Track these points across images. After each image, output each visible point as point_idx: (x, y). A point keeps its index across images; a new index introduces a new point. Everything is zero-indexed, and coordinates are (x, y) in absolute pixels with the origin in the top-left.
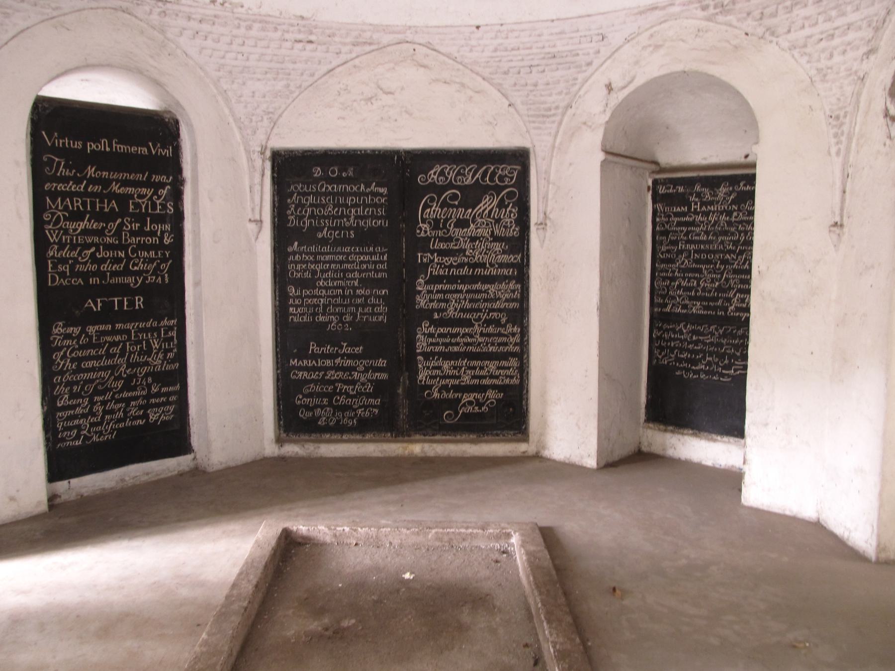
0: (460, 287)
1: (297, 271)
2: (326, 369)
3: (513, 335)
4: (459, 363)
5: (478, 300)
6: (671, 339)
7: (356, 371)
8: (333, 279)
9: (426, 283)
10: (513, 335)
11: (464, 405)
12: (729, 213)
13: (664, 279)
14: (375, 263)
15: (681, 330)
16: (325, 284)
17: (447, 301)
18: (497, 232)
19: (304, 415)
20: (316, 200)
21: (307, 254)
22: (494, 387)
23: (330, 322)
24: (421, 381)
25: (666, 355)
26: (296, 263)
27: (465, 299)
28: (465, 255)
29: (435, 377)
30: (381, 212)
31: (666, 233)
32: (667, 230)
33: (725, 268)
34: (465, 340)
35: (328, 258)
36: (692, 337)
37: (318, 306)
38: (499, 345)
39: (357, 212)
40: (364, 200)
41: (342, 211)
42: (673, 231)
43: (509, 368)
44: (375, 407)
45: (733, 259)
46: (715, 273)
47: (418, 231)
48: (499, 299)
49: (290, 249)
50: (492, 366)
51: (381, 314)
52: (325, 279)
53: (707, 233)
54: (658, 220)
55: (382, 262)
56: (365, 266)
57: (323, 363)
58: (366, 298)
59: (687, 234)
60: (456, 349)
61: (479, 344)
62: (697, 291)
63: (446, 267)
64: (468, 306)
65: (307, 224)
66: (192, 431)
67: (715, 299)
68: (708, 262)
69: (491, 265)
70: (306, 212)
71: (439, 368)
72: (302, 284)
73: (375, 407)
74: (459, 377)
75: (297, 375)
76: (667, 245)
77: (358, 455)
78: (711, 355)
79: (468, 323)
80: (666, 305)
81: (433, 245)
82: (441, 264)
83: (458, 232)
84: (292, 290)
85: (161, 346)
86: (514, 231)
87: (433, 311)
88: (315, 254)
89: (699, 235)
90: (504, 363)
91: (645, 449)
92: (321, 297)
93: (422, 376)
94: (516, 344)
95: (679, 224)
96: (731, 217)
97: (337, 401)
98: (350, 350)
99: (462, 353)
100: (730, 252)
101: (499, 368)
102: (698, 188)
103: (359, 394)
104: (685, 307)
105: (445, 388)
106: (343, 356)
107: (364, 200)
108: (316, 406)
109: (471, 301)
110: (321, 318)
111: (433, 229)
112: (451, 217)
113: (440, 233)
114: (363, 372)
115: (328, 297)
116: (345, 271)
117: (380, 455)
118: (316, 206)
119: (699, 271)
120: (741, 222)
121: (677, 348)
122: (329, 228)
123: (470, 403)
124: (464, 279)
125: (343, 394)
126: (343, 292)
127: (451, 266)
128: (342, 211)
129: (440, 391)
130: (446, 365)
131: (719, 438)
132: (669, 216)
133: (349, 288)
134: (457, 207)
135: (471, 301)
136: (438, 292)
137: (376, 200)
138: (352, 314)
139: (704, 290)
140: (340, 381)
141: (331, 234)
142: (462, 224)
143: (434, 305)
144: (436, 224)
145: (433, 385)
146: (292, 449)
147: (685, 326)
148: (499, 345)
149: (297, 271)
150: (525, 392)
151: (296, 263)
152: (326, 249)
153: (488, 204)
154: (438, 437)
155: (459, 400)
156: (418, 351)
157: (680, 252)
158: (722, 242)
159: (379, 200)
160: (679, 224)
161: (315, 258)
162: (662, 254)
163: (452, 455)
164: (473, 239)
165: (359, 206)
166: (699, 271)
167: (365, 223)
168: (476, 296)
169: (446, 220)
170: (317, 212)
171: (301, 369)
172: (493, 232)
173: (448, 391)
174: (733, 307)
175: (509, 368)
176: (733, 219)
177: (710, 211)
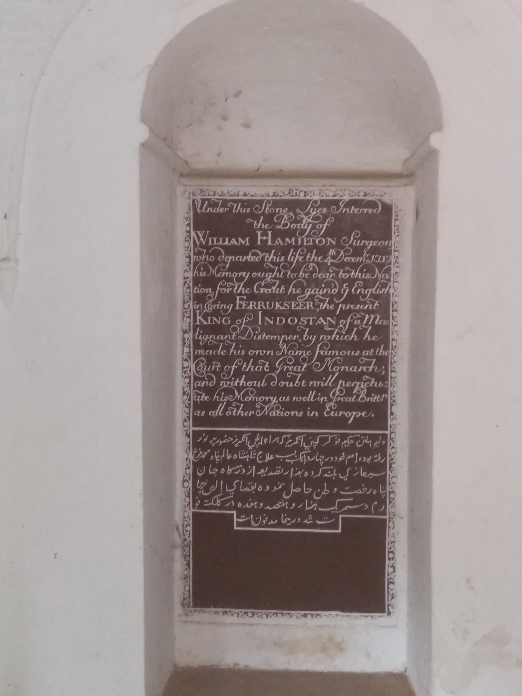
6: (225, 463)
12: (322, 251)
15: (243, 446)
25: (217, 492)
31: (210, 282)
32: (213, 276)
33: (317, 341)
36: (263, 457)
42: (225, 278)
45: (331, 325)
46: (302, 349)
53: (285, 282)
59: (250, 283)
62: (268, 381)
67: (305, 392)
68: (288, 330)
78: (298, 482)
80: (214, 405)
95: (235, 267)
96: (325, 257)
100: (325, 313)
120: (342, 265)
121: (239, 477)
132: (217, 253)
139: (282, 376)
157: (241, 313)
160: (235, 267)
166: (273, 345)
177: (290, 246)
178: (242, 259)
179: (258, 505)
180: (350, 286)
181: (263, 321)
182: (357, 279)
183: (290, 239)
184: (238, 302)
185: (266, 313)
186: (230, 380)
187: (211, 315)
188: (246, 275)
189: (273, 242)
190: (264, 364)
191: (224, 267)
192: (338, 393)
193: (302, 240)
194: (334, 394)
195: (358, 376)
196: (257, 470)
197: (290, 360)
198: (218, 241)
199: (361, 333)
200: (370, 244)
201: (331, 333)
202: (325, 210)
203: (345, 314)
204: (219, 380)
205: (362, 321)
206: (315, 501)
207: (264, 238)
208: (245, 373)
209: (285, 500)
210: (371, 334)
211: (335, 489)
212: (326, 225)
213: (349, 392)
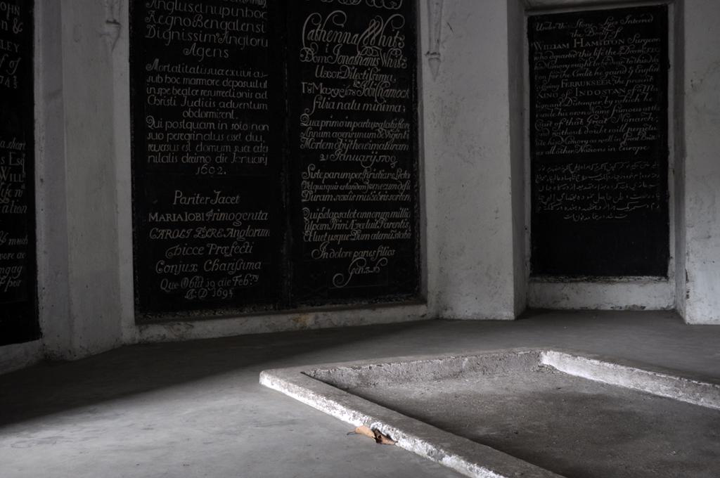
0: (348, 124)
1: (158, 97)
2: (195, 225)
3: (404, 181)
4: (348, 214)
5: (366, 141)
7: (233, 227)
8: (204, 109)
9: (312, 118)
10: (404, 181)
11: (354, 266)
12: (616, 48)
13: (546, 120)
14: (254, 90)
15: (567, 172)
16: (194, 114)
17: (334, 140)
18: (384, 62)
19: (168, 287)
20: (182, 7)
21: (170, 75)
22: (385, 242)
23: (200, 164)
24: (307, 238)
25: (552, 201)
26: (157, 86)
27: (353, 139)
28: (352, 87)
29: (320, 233)
30: (261, 29)
34: (353, 187)
35: (197, 81)
36: (580, 178)
37: (185, 142)
38: (390, 192)
39: (231, 26)
40: (240, 12)
41: (214, 23)
43: (399, 220)
44: (255, 272)
46: (603, 109)
47: (302, 55)
48: (388, 139)
49: (149, 68)
50: (382, 217)
51: (260, 155)
52: (194, 109)
53: (592, 69)
54: (535, 58)
55: (262, 91)
56: (241, 95)
57: (192, 217)
58: (244, 133)
60: (345, 198)
61: (370, 191)
62: (583, 131)
63: (332, 99)
64: (356, 146)
65: (171, 35)
66: (40, 305)
67: (605, 136)
68: (595, 98)
69: (380, 100)
70: (169, 20)
71: (327, 221)
72: (163, 113)
73: (255, 272)
74: (348, 232)
75: (158, 234)
76: (547, 85)
77: (241, 332)
79: (356, 167)
80: (549, 148)
81: (319, 74)
82: (327, 96)
83: (345, 60)
84: (152, 122)
85: (8, 178)
86: (402, 62)
87: (320, 151)
88: (181, 76)
89: (583, 71)
90: (395, 214)
91: (531, 305)
92: (187, 131)
93: (309, 230)
94: (406, 192)
95: (560, 62)
97: (209, 266)
98: (224, 200)
99: (352, 202)
100: (618, 86)
101: (390, 220)
102: (580, 23)
103: (236, 256)
104: (571, 147)
105: (333, 245)
106: (215, 208)
107: (240, 12)
108: (183, 275)
109: (361, 141)
110: (189, 159)
111: (317, 55)
112: (337, 43)
113: (326, 59)
114: (239, 228)
115: (198, 131)
116: (218, 99)
117: (269, 331)
118: (182, 14)
119: (586, 108)
120: (629, 56)
122: (199, 45)
123: (361, 262)
124: (352, 115)
125: (216, 257)
126: (216, 126)
127: (337, 99)
128: (214, 23)
129: (328, 250)
130: (334, 217)
131: (617, 279)
133: (223, 121)
134: (343, 30)
135: (361, 141)
136: (325, 129)
137: (254, 14)
138: (226, 154)
139: (592, 127)
140: (213, 240)
141: (200, 52)
142: (349, 50)
143: (320, 145)
144: (321, 48)
145: (321, 243)
146: (158, 332)
147: (573, 168)
148: (390, 192)
149: (158, 97)
150: (417, 247)
151: (157, 86)
152: (195, 70)
153: (375, 30)
154: (326, 306)
155: (349, 259)
156: (304, 200)
157: (563, 91)
158: (609, 77)
159: (258, 14)
161: (181, 80)
162: (542, 94)
163: (349, 324)
164: (361, 69)
165: (234, 19)
167: (242, 41)
168: (365, 136)
169: (333, 44)
170: (182, 21)
171: (163, 225)
172: (380, 61)
173: (337, 250)
174: (624, 142)
175: (399, 220)
176: (620, 53)
177: (595, 46)
178: (564, 56)
179: (578, 208)
180: (635, 68)
181: (579, 93)
182: (639, 64)
183: (595, 42)
184: (562, 83)
185: (580, 89)
186: (558, 132)
187: (546, 92)
188: (567, 66)
189: (584, 43)
190: (580, 121)
191: (554, 62)
192: (627, 136)
193: (603, 43)
194: (625, 137)
195: (640, 125)
196: (577, 186)
197: (596, 117)
198: (549, 47)
199: (642, 97)
200: (646, 41)
201: (623, 98)
202: (617, 23)
203: (631, 86)
204: (551, 132)
205: (643, 89)
206: (614, 204)
207: (578, 43)
208: (568, 126)
209: (595, 204)
210: (648, 97)
211: (627, 197)
212: (618, 31)
213: (635, 134)
